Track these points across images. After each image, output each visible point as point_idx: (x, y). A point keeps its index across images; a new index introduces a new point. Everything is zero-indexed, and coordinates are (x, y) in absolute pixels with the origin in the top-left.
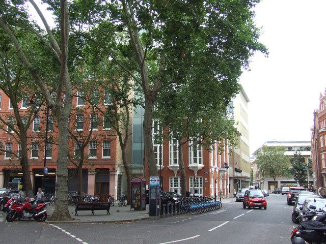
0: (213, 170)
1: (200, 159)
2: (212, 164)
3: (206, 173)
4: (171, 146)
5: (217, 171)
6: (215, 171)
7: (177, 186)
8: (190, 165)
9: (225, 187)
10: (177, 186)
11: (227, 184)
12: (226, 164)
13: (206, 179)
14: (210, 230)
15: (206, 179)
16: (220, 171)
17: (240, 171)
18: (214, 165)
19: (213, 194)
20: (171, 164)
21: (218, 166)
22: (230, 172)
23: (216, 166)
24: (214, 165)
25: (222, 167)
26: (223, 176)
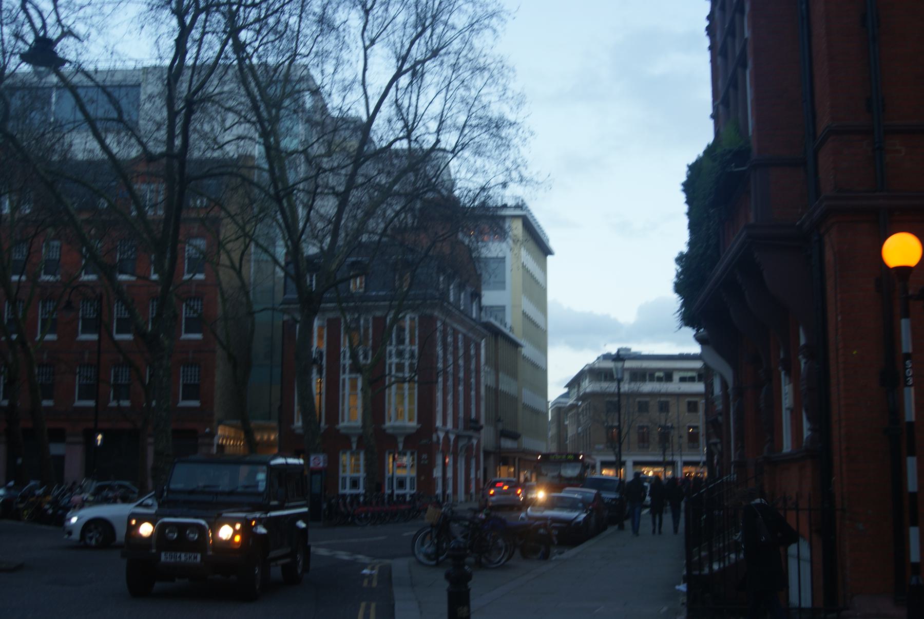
0: (441, 435)
1: (411, 412)
2: (439, 423)
3: (424, 441)
4: (344, 380)
5: (452, 437)
6: (446, 437)
7: (358, 471)
8: (388, 424)
9: (473, 476)
10: (358, 471)
11: (477, 468)
12: (477, 421)
13: (424, 456)
14: (99, 443)
15: (424, 456)
16: (458, 437)
17: (515, 437)
18: (445, 423)
19: (439, 491)
20: (343, 420)
21: (455, 425)
22: (486, 437)
23: (450, 425)
24: (445, 423)
25: (466, 428)
26: (469, 448)
